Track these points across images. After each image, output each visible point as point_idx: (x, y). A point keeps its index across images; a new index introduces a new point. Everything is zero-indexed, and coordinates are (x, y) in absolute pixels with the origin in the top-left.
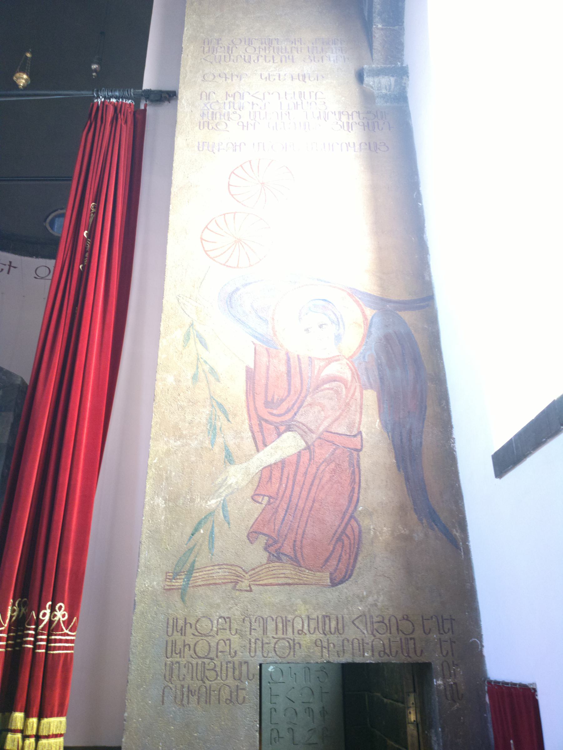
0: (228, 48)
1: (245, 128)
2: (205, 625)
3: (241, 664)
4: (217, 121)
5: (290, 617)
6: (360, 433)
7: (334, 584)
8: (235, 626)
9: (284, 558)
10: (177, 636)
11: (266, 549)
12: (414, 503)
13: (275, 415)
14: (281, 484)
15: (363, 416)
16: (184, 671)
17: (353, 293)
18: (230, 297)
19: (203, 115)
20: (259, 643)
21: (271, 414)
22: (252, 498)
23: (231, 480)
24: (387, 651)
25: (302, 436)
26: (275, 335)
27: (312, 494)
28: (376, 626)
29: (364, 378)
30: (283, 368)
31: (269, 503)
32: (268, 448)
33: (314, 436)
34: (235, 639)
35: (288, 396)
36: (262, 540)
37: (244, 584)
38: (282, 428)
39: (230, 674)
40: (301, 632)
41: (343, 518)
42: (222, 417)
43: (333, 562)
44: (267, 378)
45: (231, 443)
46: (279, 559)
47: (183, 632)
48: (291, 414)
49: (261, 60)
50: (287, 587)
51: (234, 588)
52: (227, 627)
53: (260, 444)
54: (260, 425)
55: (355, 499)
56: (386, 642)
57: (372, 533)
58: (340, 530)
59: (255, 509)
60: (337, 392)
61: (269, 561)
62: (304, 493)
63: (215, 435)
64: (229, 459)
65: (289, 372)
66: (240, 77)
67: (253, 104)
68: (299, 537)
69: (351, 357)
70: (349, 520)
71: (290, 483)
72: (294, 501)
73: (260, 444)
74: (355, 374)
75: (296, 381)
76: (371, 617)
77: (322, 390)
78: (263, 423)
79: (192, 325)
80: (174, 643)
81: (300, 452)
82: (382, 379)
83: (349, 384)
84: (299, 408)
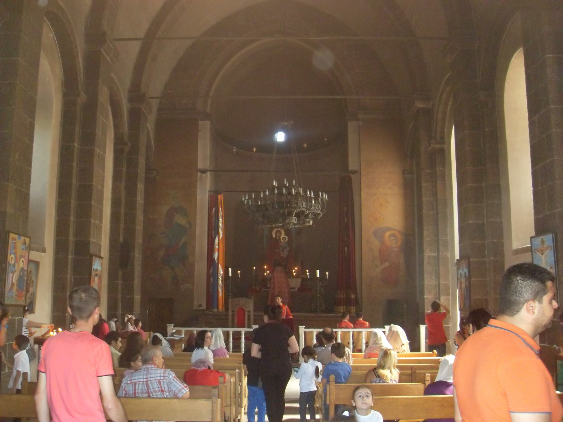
17: (399, 232)
64: (376, 267)
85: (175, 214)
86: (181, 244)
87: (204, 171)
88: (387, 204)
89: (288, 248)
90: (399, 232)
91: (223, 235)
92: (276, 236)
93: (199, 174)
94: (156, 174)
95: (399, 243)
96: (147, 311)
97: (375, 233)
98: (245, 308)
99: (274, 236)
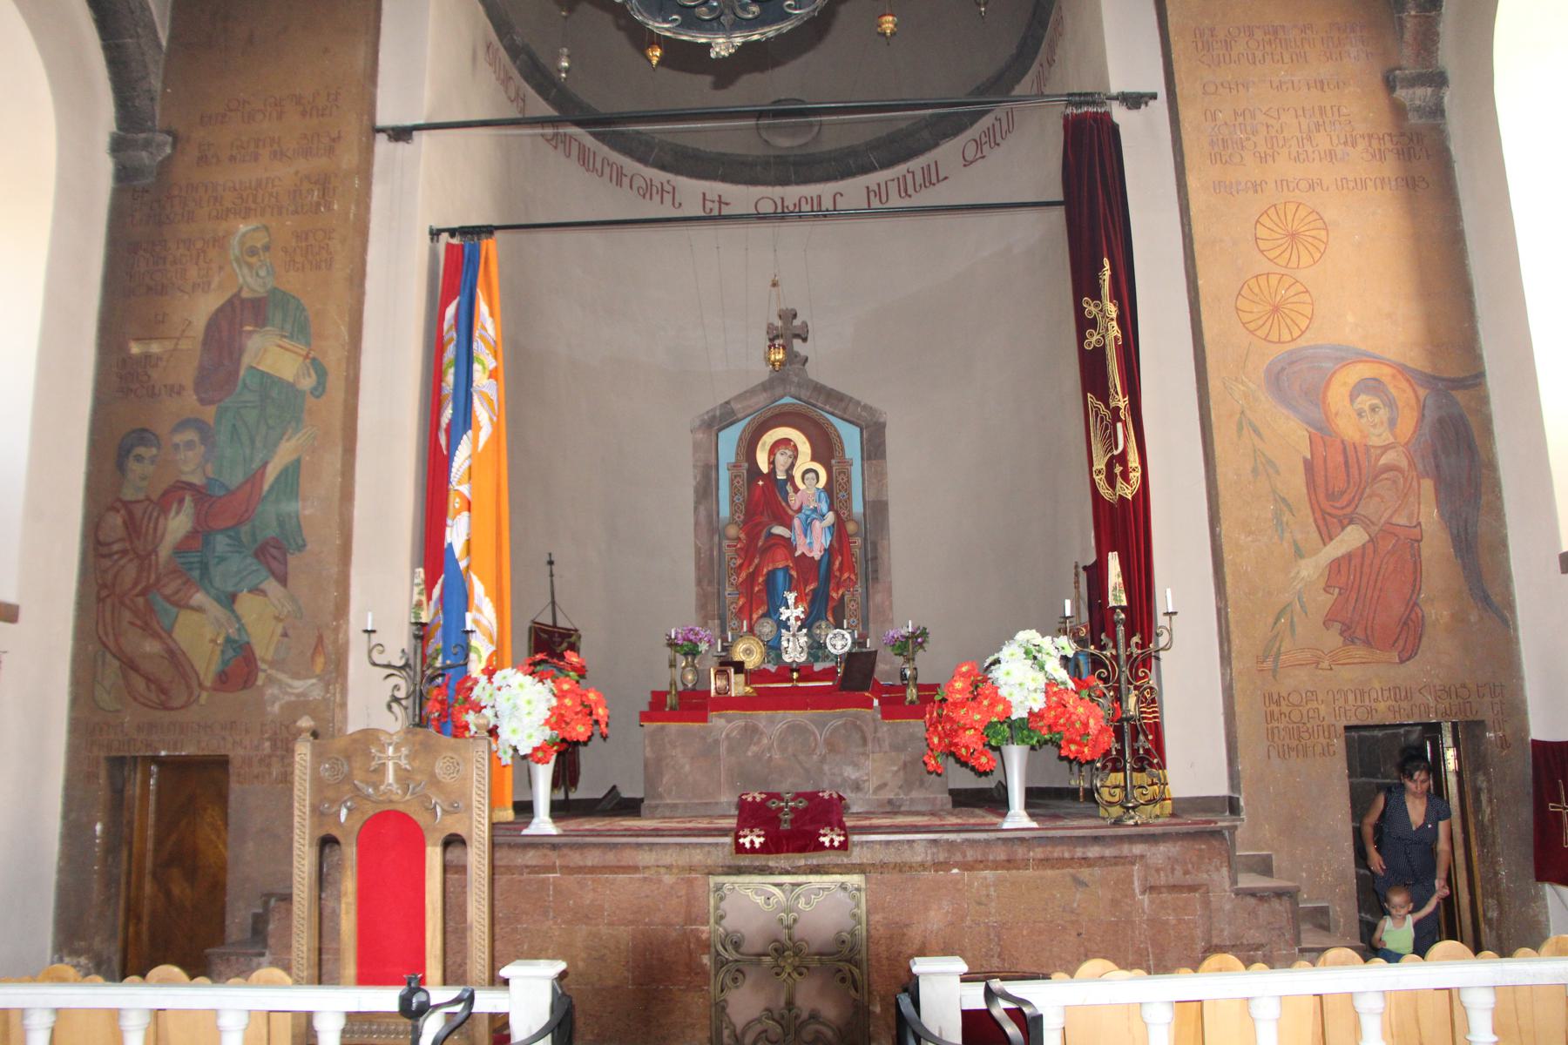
0: (1226, 41)
1: (1264, 160)
2: (1295, 698)
3: (1329, 727)
4: (1230, 151)
5: (1366, 689)
6: (1419, 524)
7: (1402, 662)
8: (1320, 697)
9: (1356, 640)
10: (1274, 707)
11: (1341, 634)
12: (1471, 589)
13: (1337, 508)
14: (1348, 578)
15: (1422, 506)
16: (1283, 733)
18: (1278, 376)
19: (1212, 143)
20: (1342, 710)
21: (1332, 506)
22: (1325, 590)
23: (1304, 573)
24: (1448, 712)
25: (1365, 529)
26: (1328, 421)
27: (1379, 584)
28: (1439, 693)
29: (1420, 467)
30: (1340, 459)
31: (1340, 594)
32: (1334, 541)
33: (1377, 528)
34: (1322, 708)
35: (1348, 488)
36: (1338, 626)
37: (1325, 664)
38: (1346, 522)
39: (1321, 733)
40: (1376, 700)
41: (1407, 605)
42: (1287, 513)
43: (1401, 642)
44: (1326, 469)
45: (1299, 537)
46: (1353, 642)
47: (1278, 703)
48: (1353, 506)
49: (1268, 58)
50: (1363, 666)
51: (1317, 667)
52: (1314, 698)
53: (1327, 540)
54: (1324, 519)
55: (1418, 587)
56: (1448, 706)
57: (1434, 617)
58: (1405, 616)
59: (1325, 600)
60: (1394, 482)
61: (1345, 645)
62: (1371, 583)
63: (1283, 530)
64: (1299, 554)
65: (1346, 463)
66: (1246, 86)
67: (1268, 127)
68: (1369, 623)
69: (1406, 444)
70: (1413, 607)
71: (1358, 575)
72: (1363, 591)
73: (1327, 540)
74: (1412, 464)
75: (1354, 471)
76: (1435, 686)
77: (1381, 480)
78: (1326, 516)
79: (1243, 412)
80: (1272, 714)
81: (1364, 545)
82: (1437, 466)
83: (1406, 473)
84: (1360, 499)
85: (248, 328)
86: (272, 473)
87: (401, 134)
88: (1323, 233)
89: (830, 517)
90: (1402, 370)
91: (496, 427)
92: (772, 463)
93: (382, 144)
94: (168, 150)
95: (1407, 423)
96: (99, 827)
97: (1276, 380)
98: (421, 818)
99: (764, 467)
